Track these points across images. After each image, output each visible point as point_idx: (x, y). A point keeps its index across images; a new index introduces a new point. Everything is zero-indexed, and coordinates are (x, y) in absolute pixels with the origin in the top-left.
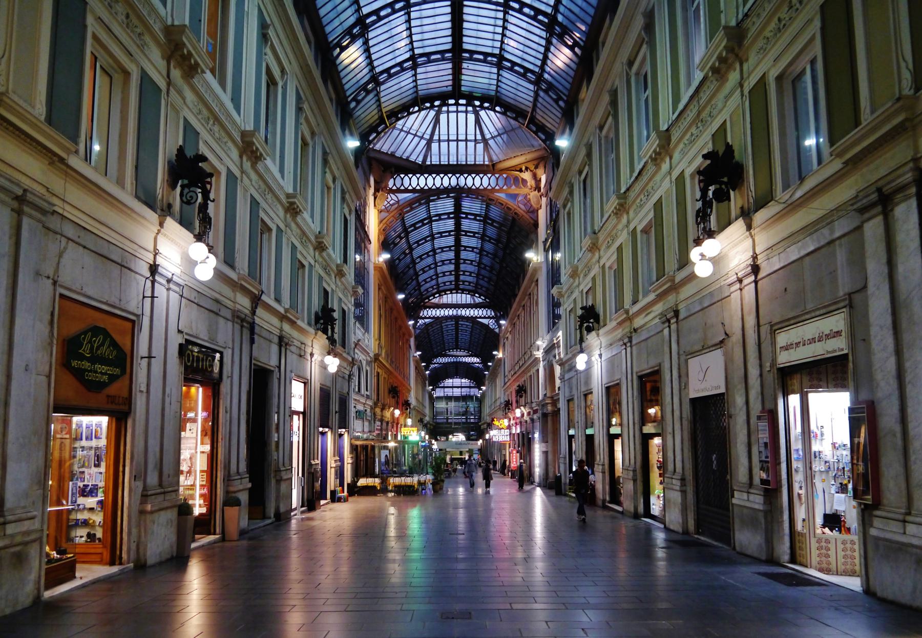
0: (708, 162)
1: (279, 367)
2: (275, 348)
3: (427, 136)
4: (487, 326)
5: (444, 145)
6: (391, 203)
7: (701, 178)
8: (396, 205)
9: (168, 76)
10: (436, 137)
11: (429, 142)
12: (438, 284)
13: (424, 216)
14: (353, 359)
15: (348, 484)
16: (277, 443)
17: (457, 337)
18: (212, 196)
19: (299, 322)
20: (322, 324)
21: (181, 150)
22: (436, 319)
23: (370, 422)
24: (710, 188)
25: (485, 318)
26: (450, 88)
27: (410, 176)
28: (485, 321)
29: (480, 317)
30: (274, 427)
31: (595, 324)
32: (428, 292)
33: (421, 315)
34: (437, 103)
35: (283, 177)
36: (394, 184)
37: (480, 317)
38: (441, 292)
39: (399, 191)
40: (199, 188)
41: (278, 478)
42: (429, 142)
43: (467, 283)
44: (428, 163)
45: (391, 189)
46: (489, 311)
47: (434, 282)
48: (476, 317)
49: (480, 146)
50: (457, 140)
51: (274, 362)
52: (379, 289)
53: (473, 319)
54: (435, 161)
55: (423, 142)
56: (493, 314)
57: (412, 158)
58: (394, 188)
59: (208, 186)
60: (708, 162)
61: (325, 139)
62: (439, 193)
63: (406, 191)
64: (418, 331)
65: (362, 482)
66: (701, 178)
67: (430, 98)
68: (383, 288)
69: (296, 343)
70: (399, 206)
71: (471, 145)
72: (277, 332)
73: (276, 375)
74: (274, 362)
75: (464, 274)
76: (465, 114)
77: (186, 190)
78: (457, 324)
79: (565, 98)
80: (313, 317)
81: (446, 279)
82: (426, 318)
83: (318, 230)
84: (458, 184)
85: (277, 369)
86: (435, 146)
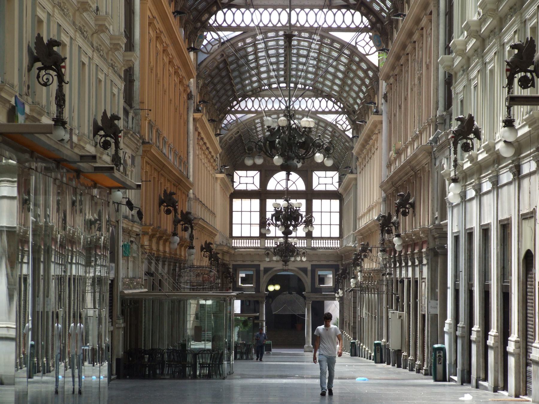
0: (516, 51)
4: (353, 50)
7: (508, 67)
15: (118, 360)
17: (288, 63)
18: (67, 79)
24: (516, 75)
25: (348, 29)
28: (347, 37)
29: (339, 29)
33: (211, 21)
37: (339, 29)
40: (54, 70)
46: (358, 14)
48: (330, 29)
59: (63, 70)
60: (516, 51)
64: (202, 57)
66: (508, 67)
77: (43, 72)
80: (91, 128)
82: (220, 28)
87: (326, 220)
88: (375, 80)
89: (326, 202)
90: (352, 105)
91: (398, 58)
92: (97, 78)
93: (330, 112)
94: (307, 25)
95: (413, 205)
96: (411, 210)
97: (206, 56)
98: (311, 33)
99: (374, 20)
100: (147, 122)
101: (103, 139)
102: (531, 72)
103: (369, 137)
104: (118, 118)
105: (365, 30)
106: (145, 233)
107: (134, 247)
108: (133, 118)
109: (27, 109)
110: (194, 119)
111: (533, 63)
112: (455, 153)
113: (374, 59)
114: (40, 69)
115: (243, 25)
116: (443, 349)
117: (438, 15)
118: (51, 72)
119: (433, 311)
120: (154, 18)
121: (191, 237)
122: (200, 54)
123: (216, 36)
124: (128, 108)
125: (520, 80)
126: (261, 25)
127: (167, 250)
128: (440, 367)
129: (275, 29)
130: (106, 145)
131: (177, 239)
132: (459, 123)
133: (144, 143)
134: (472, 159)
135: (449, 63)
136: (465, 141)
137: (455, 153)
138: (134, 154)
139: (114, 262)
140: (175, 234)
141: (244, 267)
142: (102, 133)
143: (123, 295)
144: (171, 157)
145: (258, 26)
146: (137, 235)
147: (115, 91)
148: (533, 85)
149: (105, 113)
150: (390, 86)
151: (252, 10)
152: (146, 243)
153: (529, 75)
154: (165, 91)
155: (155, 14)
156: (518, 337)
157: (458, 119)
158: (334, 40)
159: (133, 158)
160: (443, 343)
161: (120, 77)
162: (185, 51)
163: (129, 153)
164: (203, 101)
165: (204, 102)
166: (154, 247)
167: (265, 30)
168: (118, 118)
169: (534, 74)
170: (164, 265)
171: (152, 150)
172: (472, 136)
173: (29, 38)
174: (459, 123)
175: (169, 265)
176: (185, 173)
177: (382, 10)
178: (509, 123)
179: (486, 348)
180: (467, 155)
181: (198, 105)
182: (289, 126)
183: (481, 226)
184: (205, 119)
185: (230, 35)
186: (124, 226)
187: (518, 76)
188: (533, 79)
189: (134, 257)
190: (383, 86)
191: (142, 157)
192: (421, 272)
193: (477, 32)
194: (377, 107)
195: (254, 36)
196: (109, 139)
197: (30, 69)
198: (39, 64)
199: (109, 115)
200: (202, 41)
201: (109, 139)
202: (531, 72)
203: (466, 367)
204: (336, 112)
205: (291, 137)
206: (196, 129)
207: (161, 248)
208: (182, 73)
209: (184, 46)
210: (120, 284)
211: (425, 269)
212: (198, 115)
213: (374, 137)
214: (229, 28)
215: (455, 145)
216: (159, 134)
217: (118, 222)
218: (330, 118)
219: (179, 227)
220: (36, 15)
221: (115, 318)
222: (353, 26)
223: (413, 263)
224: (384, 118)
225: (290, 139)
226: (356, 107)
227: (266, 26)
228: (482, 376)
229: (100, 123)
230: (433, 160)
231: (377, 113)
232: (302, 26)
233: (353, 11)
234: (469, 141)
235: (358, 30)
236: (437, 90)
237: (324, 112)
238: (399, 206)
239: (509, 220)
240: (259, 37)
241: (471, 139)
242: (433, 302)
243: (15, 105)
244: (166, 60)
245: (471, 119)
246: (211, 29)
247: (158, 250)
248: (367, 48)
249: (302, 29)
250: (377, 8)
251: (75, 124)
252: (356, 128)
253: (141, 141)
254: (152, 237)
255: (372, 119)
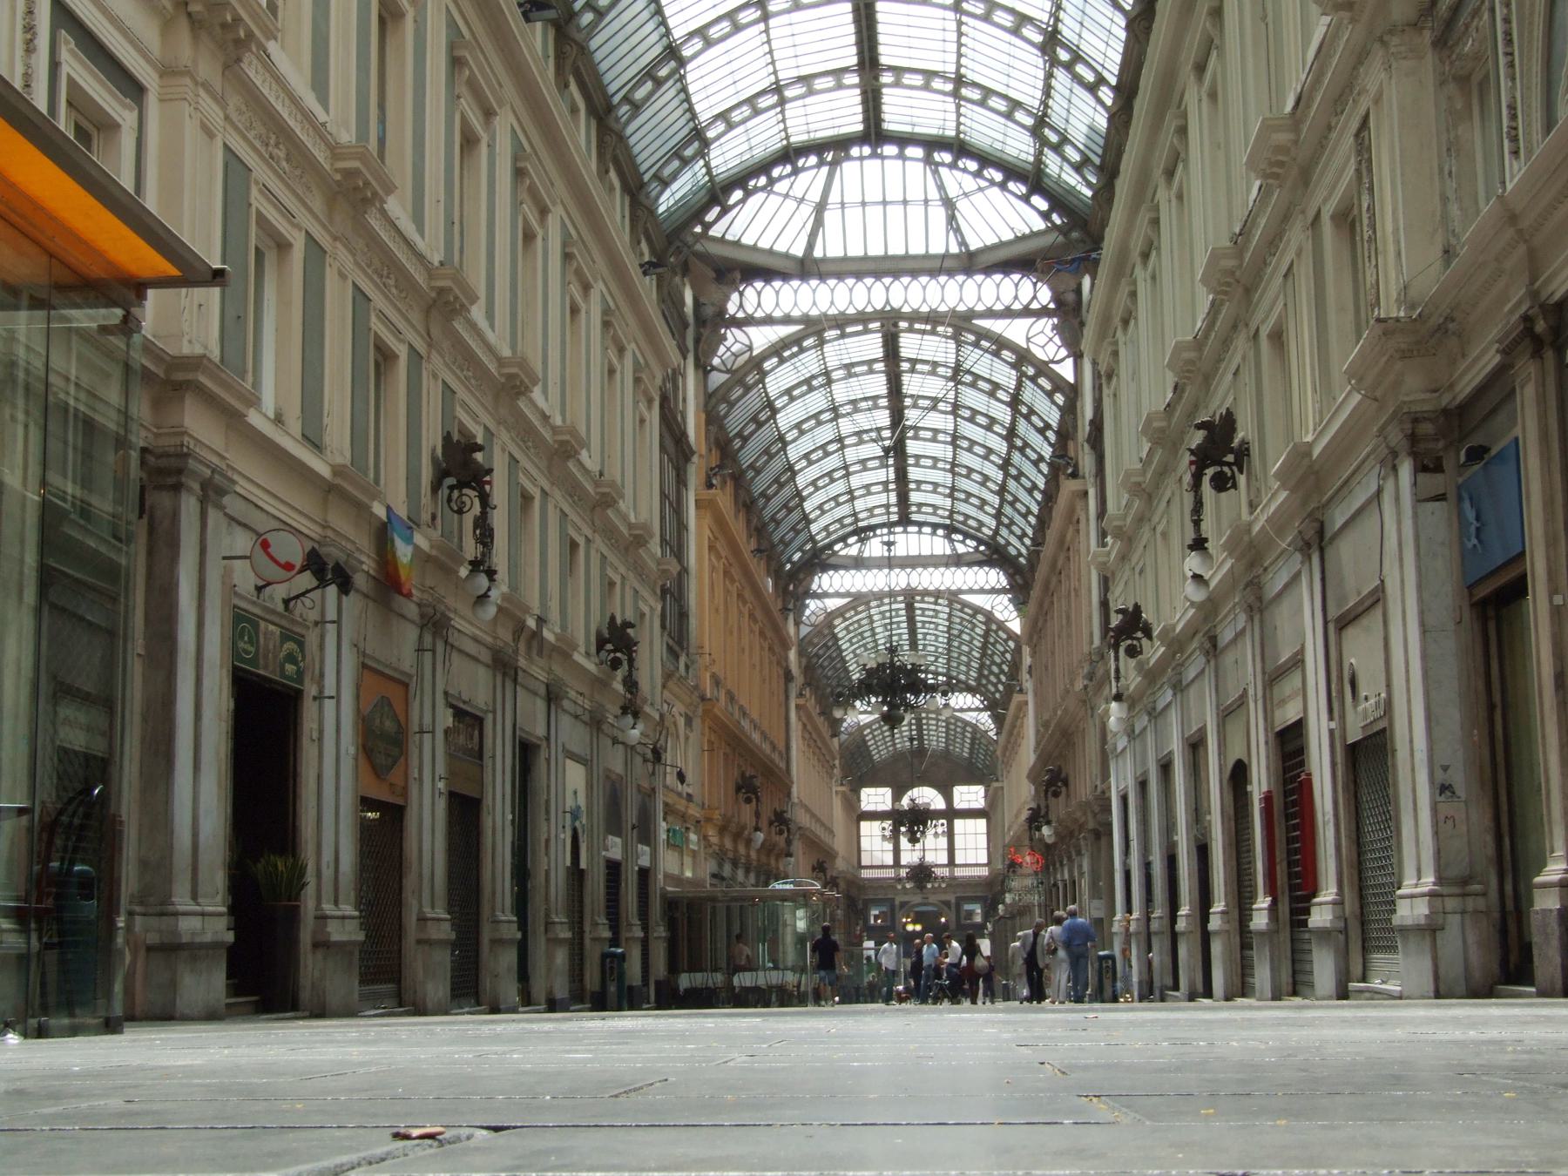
1: (548, 739)
2: (540, 705)
3: (815, 195)
4: (989, 617)
5: (853, 214)
6: (734, 349)
7: (1193, 458)
8: (748, 354)
9: (429, 334)
10: (834, 197)
11: (820, 208)
12: (855, 514)
13: (815, 368)
14: (662, 716)
15: (658, 983)
16: (547, 873)
19: (579, 658)
20: (610, 652)
21: (447, 438)
22: (859, 600)
23: (694, 854)
24: (1207, 471)
25: (982, 591)
26: (860, 127)
27: (777, 284)
29: (971, 591)
30: (543, 844)
31: (1145, 641)
32: (829, 534)
33: (814, 587)
34: (829, 157)
35: (547, 399)
36: (741, 306)
37: (971, 591)
38: (863, 533)
39: (750, 321)
40: (474, 489)
41: (551, 935)
42: (820, 208)
43: (930, 510)
44: (818, 253)
45: (733, 318)
47: (845, 510)
48: (960, 591)
49: (938, 214)
50: (885, 203)
51: (540, 731)
52: (711, 548)
53: (953, 597)
54: (835, 251)
55: (807, 210)
56: (1004, 582)
57: (780, 247)
58: (740, 315)
59: (487, 487)
61: (606, 284)
62: (841, 322)
63: (769, 320)
64: (804, 630)
65: (685, 981)
66: (1193, 458)
67: (818, 148)
68: (718, 545)
69: (572, 694)
70: (751, 358)
71: (916, 212)
72: (542, 676)
73: (543, 754)
74: (540, 731)
75: (918, 489)
76: (881, 207)
77: (456, 493)
78: (910, 608)
79: (1097, 161)
80: (593, 639)
81: (872, 501)
82: (825, 595)
83: (598, 468)
84: (888, 302)
85: (544, 744)
86: (831, 217)
87: (971, 845)
88: (1018, 651)
89: (970, 822)
90: (993, 694)
91: (1041, 605)
92: (603, 575)
93: (970, 709)
94: (931, 588)
95: (1066, 783)
96: (1064, 789)
97: (809, 629)
98: (937, 597)
99: (1011, 571)
100: (708, 675)
101: (612, 655)
102: (1229, 464)
103: (1013, 726)
104: (632, 626)
105: (1003, 591)
106: (709, 820)
107: (693, 837)
108: (687, 667)
109: (419, 539)
110: (798, 706)
111: (1231, 451)
112: (1117, 659)
113: (1016, 626)
114: (451, 488)
115: (853, 590)
116: (1112, 958)
117: (1088, 520)
118: (472, 493)
119: (1097, 914)
120: (716, 539)
121: (789, 842)
122: (802, 626)
123: (821, 605)
124: (677, 648)
125: (1213, 479)
126: (875, 589)
127: (753, 855)
128: (1107, 983)
129: (892, 594)
130: (615, 664)
131: (760, 837)
132: (1120, 616)
133: (703, 698)
134: (1140, 668)
135: (1105, 559)
136: (1129, 642)
137: (1117, 659)
138: (690, 714)
139: (648, 844)
140: (757, 829)
141: (877, 902)
142: (609, 647)
143: (664, 895)
144: (756, 737)
145: (871, 591)
146: (698, 822)
147: (646, 610)
148: (1235, 486)
149: (613, 618)
150: (1033, 654)
151: (864, 572)
152: (712, 832)
153: (1226, 469)
154: (743, 649)
155: (717, 535)
156: (1227, 905)
157: (1119, 611)
158: (965, 605)
159: (689, 721)
160: (1111, 947)
161: (655, 593)
162: (777, 615)
163: (678, 708)
164: (808, 684)
165: (809, 684)
166: (728, 844)
167: (879, 596)
168: (632, 626)
169: (1235, 468)
170: (747, 871)
171: (716, 710)
172: (1139, 634)
173: (431, 439)
174: (1120, 616)
175: (757, 877)
176: (783, 765)
177: (1020, 554)
178: (1199, 544)
179: (1174, 937)
180: (1132, 663)
181: (801, 690)
182: (892, 664)
183: (1158, 761)
184: (815, 710)
185: (839, 602)
186: (669, 801)
187: (1210, 472)
188: (1233, 477)
189: (694, 851)
190: (1026, 650)
191: (703, 721)
192: (1080, 866)
193: (1139, 484)
194: (1021, 685)
195: (867, 603)
196: (618, 655)
197: (436, 487)
198: (451, 481)
199: (619, 621)
200: (804, 612)
201: (618, 655)
202: (1229, 464)
203: (1145, 977)
204: (977, 709)
205: (894, 679)
206: (799, 719)
207: (742, 850)
208: (777, 649)
209: (776, 606)
210: (661, 877)
211: (1086, 867)
212: (801, 701)
213: (1018, 723)
214: (838, 595)
215: (1116, 647)
216: (731, 697)
217: (653, 790)
218: (969, 717)
219: (773, 829)
220: (455, 417)
221: (652, 923)
222: (987, 587)
223: (1070, 859)
224: (1030, 698)
225: (893, 681)
226: (997, 695)
227: (881, 590)
228: (1169, 981)
229: (606, 634)
230: (1089, 711)
231: (1021, 691)
232: (926, 590)
233: (987, 569)
234: (1135, 642)
235: (993, 591)
236: (1090, 617)
237: (962, 710)
238: (1050, 784)
239: (1202, 731)
240: (873, 604)
241: (1139, 639)
242: (1096, 903)
243: (385, 519)
244: (756, 628)
245: (1137, 608)
246: (816, 596)
247: (736, 850)
248: (1006, 613)
249: (926, 593)
250: (1013, 552)
251: (554, 615)
252: (998, 720)
253: (696, 693)
254: (722, 830)
255: (1017, 698)
